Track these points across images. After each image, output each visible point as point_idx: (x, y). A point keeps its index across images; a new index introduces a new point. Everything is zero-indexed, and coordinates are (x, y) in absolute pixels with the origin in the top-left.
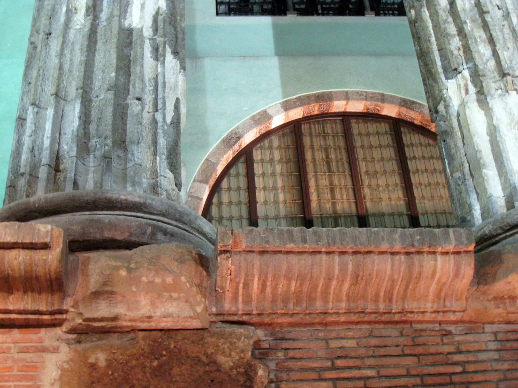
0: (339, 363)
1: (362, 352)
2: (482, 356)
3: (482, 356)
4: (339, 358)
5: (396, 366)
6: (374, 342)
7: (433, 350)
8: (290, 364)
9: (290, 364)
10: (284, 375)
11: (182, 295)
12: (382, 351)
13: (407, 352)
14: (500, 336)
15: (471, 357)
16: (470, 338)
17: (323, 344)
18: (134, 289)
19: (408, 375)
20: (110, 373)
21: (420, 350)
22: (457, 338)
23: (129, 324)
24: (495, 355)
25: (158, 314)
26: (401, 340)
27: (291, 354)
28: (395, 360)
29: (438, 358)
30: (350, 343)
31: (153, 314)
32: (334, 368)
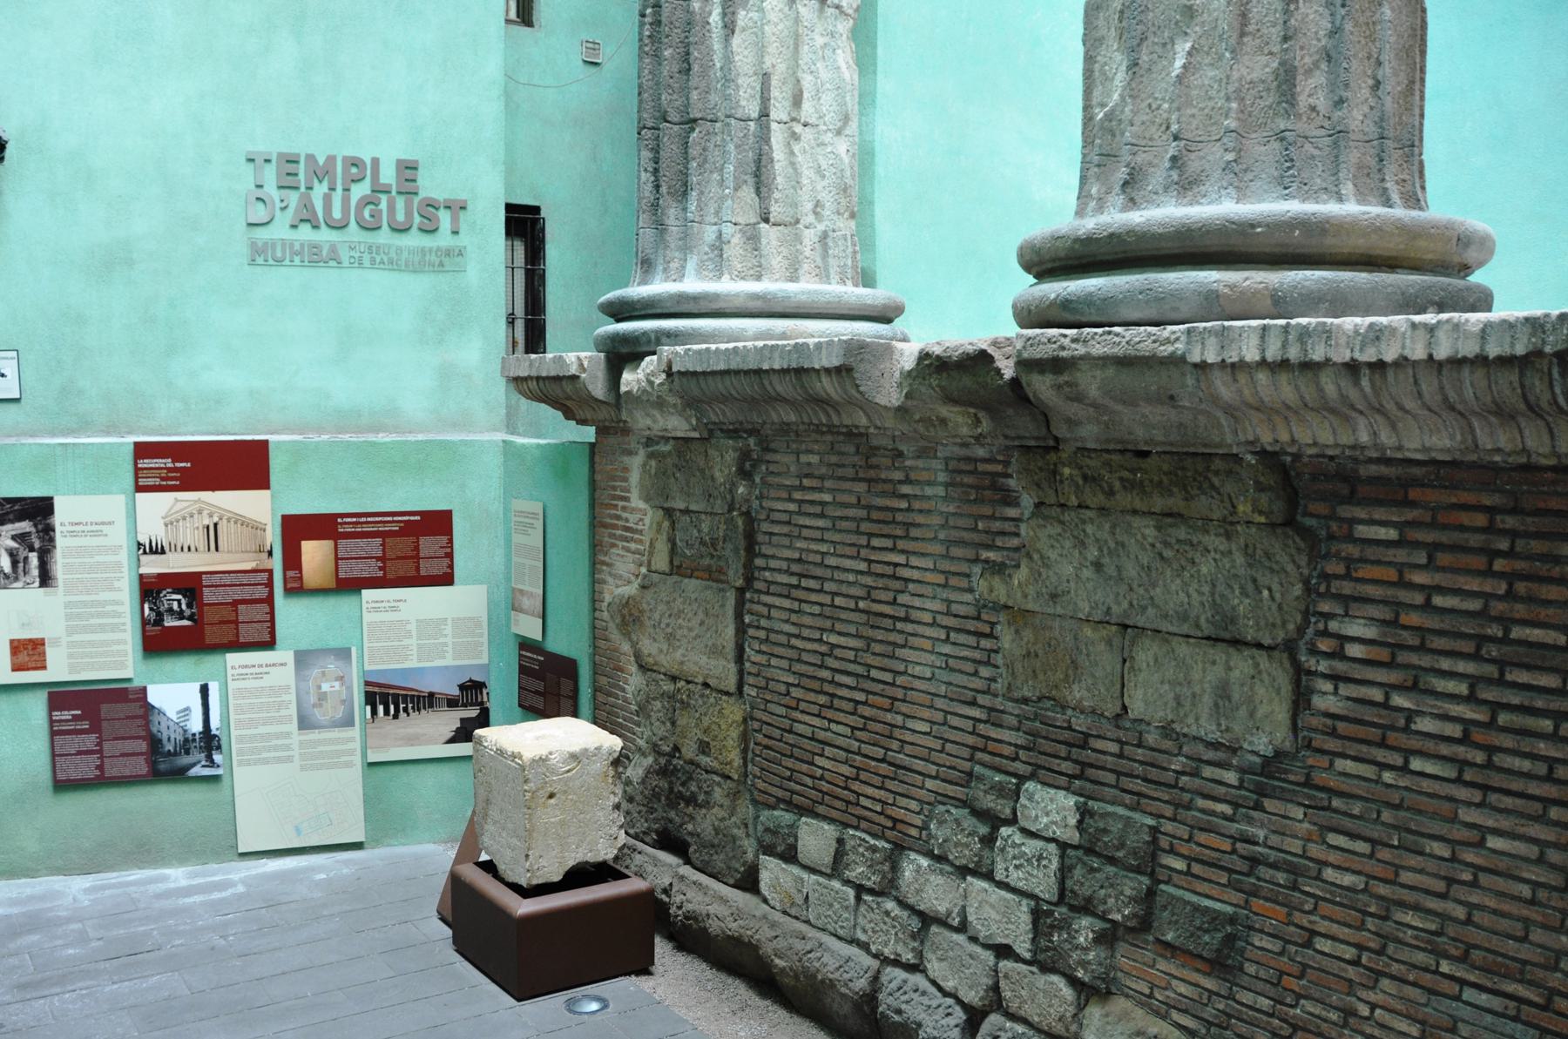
1: (823, 470)
2: (929, 491)
3: (929, 491)
4: (807, 476)
5: (850, 492)
6: (834, 459)
7: (883, 476)
8: (771, 479)
9: (771, 479)
12: (840, 472)
13: (861, 475)
14: (952, 465)
16: (920, 463)
19: (858, 505)
21: (872, 473)
22: (908, 463)
24: (941, 491)
26: (856, 459)
28: (847, 485)
30: (814, 459)
32: (802, 488)
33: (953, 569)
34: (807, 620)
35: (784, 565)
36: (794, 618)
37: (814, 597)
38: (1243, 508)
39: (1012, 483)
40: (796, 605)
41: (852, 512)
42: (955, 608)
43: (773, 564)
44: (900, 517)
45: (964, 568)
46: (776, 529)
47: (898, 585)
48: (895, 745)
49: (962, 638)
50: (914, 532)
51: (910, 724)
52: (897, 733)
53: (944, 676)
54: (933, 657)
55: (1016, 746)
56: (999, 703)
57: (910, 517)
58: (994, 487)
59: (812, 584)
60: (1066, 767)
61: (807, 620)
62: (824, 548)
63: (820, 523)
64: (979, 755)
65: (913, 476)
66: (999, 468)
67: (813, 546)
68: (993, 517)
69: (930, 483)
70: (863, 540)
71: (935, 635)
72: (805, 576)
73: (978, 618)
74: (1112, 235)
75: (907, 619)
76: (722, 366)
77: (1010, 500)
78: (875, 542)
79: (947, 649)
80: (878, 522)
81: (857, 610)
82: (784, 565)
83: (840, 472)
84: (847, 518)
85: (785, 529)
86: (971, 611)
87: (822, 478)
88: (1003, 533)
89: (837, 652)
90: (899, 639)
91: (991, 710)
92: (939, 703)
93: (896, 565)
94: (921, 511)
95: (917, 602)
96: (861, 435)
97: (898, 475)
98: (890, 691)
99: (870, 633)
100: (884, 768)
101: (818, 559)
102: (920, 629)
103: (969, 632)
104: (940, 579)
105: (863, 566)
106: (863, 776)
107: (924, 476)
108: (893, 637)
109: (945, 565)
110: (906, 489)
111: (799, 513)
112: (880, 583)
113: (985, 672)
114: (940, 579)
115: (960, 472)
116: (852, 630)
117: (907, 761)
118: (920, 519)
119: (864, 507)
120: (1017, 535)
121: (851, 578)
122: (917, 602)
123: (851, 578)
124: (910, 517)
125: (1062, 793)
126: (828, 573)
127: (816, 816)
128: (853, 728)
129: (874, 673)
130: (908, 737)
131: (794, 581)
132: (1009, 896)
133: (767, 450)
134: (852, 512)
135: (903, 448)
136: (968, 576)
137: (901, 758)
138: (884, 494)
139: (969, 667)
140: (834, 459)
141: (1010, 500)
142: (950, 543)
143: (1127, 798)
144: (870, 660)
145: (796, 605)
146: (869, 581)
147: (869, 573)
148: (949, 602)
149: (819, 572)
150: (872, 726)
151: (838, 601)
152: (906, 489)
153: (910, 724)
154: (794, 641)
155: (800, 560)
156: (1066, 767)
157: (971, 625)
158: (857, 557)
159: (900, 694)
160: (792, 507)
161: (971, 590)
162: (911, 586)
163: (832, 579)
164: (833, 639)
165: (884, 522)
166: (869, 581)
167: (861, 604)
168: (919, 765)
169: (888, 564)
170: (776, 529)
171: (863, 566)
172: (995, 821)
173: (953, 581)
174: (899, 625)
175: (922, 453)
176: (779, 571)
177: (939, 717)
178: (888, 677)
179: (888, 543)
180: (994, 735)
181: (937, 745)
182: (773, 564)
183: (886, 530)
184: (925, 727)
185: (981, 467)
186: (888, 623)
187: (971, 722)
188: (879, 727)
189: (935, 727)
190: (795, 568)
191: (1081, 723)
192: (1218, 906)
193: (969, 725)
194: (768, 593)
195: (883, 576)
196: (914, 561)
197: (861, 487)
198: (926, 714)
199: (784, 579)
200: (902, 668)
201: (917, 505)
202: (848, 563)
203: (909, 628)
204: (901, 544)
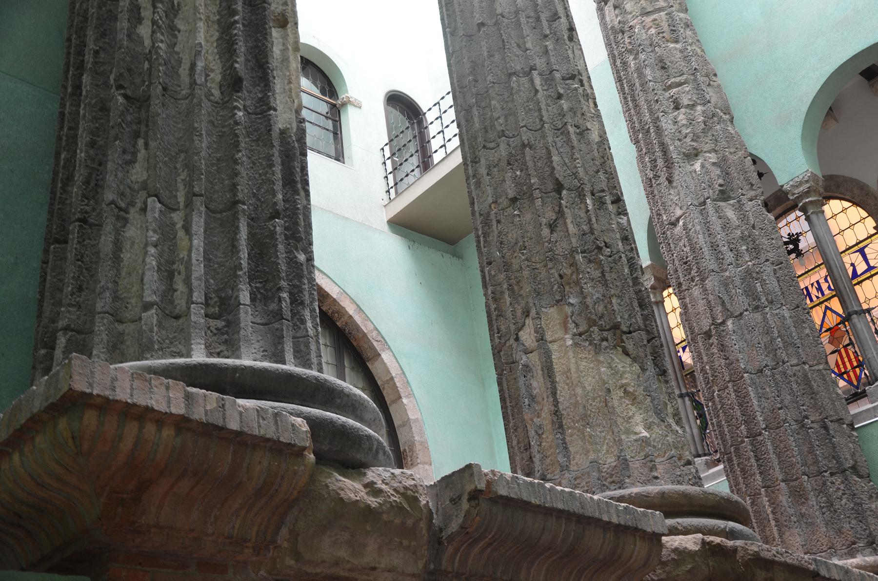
11: (413, 543)
18: (368, 528)
23: (346, 574)
25: (383, 566)
31: (377, 565)
76: (560, 506)
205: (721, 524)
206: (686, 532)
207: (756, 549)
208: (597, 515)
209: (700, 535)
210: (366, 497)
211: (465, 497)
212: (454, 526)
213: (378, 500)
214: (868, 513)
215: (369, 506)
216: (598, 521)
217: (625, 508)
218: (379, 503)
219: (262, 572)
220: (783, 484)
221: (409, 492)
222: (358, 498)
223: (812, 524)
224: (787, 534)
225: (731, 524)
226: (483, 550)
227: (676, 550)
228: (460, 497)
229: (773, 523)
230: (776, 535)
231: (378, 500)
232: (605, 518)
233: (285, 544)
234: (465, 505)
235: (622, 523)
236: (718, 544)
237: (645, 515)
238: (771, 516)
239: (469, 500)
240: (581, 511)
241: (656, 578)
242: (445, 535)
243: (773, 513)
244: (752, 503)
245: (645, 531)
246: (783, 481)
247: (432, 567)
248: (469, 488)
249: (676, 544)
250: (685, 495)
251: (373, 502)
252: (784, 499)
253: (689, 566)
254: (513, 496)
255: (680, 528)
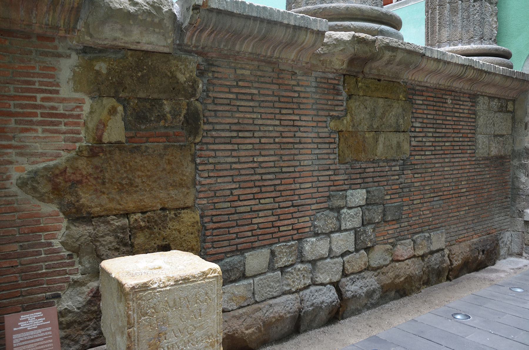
0: (240, 83)
1: (252, 78)
2: (308, 89)
3: (308, 89)
4: (240, 80)
5: (268, 89)
6: (259, 73)
7: (286, 83)
8: (215, 81)
9: (215, 81)
10: (211, 88)
11: (162, 31)
12: (262, 79)
13: (274, 81)
14: (318, 80)
15: (303, 89)
16: (304, 78)
17: (233, 71)
18: (131, 22)
19: (273, 95)
20: (110, 78)
21: (280, 81)
22: (299, 78)
23: (123, 45)
24: (313, 90)
25: (144, 41)
26: (272, 74)
27: (216, 75)
28: (268, 86)
29: (289, 87)
30: (247, 72)
31: (140, 41)
32: (237, 86)
33: (320, 120)
34: (243, 153)
35: (227, 127)
36: (234, 154)
37: (248, 141)
38: (401, 96)
39: (341, 87)
40: (236, 147)
41: (269, 98)
42: (321, 135)
43: (218, 127)
44: (295, 100)
45: (324, 119)
46: (220, 108)
47: (295, 129)
48: (296, 197)
49: (323, 146)
50: (302, 106)
51: (303, 186)
52: (297, 192)
53: (317, 162)
54: (312, 156)
55: (343, 180)
56: (338, 166)
57: (300, 100)
58: (334, 89)
59: (247, 134)
60: (359, 181)
61: (243, 153)
62: (254, 116)
63: (251, 104)
64: (332, 188)
65: (300, 83)
66: (336, 82)
67: (248, 116)
68: (333, 99)
69: (308, 86)
70: (277, 111)
71: (312, 147)
72: (240, 131)
73: (330, 137)
74: (391, 15)
75: (300, 143)
76: (254, 14)
77: (339, 94)
78: (284, 111)
79: (317, 151)
80: (284, 102)
81: (275, 143)
82: (227, 127)
83: (262, 79)
84: (266, 101)
85: (227, 108)
86: (327, 135)
87: (251, 82)
88: (337, 105)
89: (263, 165)
90: (296, 152)
91: (335, 170)
92: (315, 173)
93: (294, 120)
94: (304, 98)
95: (305, 135)
96: (275, 63)
97: (293, 83)
98: (293, 175)
99: (282, 152)
100: (292, 209)
101: (251, 121)
102: (305, 146)
103: (325, 143)
104: (314, 124)
105: (277, 123)
106: (282, 217)
107: (306, 83)
108: (293, 152)
109: (316, 119)
110: (298, 88)
111: (237, 99)
112: (286, 129)
113: (332, 156)
114: (314, 124)
115: (321, 82)
116: (272, 152)
117: (303, 202)
118: (304, 101)
119: (276, 96)
120: (342, 105)
121: (271, 128)
122: (305, 135)
123: (271, 128)
124: (300, 100)
125: (359, 190)
126: (257, 128)
127: (253, 248)
128: (274, 198)
129: (284, 170)
130: (302, 191)
131: (234, 134)
132: (346, 233)
133: (212, 65)
134: (269, 98)
135: (297, 71)
136: (325, 122)
137: (299, 202)
138: (286, 90)
139: (326, 156)
140: (259, 73)
141: (339, 94)
142: (318, 110)
143: (376, 184)
144: (282, 164)
145: (236, 147)
146: (281, 129)
147: (281, 125)
148: (318, 133)
149: (251, 128)
150: (284, 193)
151: (263, 140)
152: (298, 88)
153: (303, 186)
154: (234, 166)
155: (239, 123)
156: (359, 181)
157: (327, 140)
158: (275, 119)
159: (297, 175)
160: (231, 96)
161: (327, 127)
162: (302, 129)
163: (260, 131)
164: (261, 159)
165: (287, 102)
166: (281, 129)
167: (277, 140)
168: (309, 201)
169: (290, 120)
170: (220, 108)
171: (277, 123)
172: (338, 209)
173: (320, 124)
174: (296, 146)
175: (305, 74)
176: (223, 130)
177: (315, 179)
178: (291, 169)
179: (290, 111)
180: (337, 179)
181: (315, 190)
182: (218, 127)
183: (289, 106)
184: (309, 185)
185: (330, 81)
186: (290, 146)
187: (328, 177)
188: (288, 193)
189: (314, 184)
190: (234, 127)
191: (364, 166)
192: (398, 204)
193: (327, 178)
194: (214, 144)
195: (287, 126)
196: (303, 118)
197: (275, 87)
198: (310, 179)
199: (228, 134)
200: (298, 164)
201: (302, 95)
202: (269, 122)
203: (301, 146)
204: (296, 112)
205: (376, 26)
206: (346, 29)
207: (388, 41)
208: (280, 20)
209: (353, 33)
210: (128, 6)
211: (191, 8)
212: (186, 24)
213: (135, 8)
214: (487, 23)
215: (129, 11)
216: (281, 24)
217: (302, 17)
218: (136, 10)
219: (74, 42)
220: (448, 5)
221: (156, 4)
222: (122, 7)
223: (456, 26)
224: (443, 30)
225: (383, 27)
226: (210, 35)
227: (336, 39)
228: (189, 7)
229: (437, 24)
230: (437, 30)
231: (135, 8)
232: (286, 22)
233: (83, 29)
234: (191, 13)
235: (297, 25)
236: (363, 38)
237: (315, 21)
238: (437, 21)
239: (193, 10)
240: (269, 18)
241: (322, 52)
242: (183, 26)
243: (439, 19)
244: (431, 13)
245: (312, 29)
246: (449, 3)
247: (178, 42)
248: (193, 3)
249: (337, 36)
250: (360, 10)
251: (132, 9)
252: (446, 12)
253: (342, 48)
254: (221, 8)
255: (352, 27)
